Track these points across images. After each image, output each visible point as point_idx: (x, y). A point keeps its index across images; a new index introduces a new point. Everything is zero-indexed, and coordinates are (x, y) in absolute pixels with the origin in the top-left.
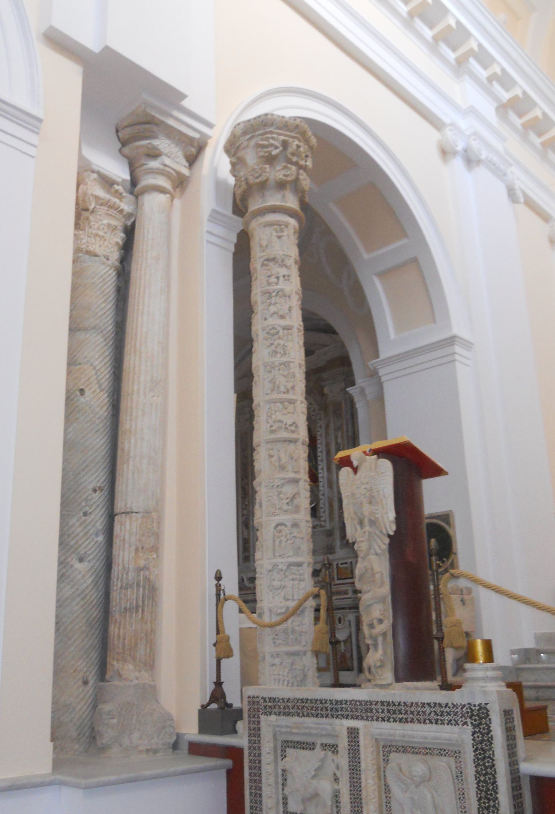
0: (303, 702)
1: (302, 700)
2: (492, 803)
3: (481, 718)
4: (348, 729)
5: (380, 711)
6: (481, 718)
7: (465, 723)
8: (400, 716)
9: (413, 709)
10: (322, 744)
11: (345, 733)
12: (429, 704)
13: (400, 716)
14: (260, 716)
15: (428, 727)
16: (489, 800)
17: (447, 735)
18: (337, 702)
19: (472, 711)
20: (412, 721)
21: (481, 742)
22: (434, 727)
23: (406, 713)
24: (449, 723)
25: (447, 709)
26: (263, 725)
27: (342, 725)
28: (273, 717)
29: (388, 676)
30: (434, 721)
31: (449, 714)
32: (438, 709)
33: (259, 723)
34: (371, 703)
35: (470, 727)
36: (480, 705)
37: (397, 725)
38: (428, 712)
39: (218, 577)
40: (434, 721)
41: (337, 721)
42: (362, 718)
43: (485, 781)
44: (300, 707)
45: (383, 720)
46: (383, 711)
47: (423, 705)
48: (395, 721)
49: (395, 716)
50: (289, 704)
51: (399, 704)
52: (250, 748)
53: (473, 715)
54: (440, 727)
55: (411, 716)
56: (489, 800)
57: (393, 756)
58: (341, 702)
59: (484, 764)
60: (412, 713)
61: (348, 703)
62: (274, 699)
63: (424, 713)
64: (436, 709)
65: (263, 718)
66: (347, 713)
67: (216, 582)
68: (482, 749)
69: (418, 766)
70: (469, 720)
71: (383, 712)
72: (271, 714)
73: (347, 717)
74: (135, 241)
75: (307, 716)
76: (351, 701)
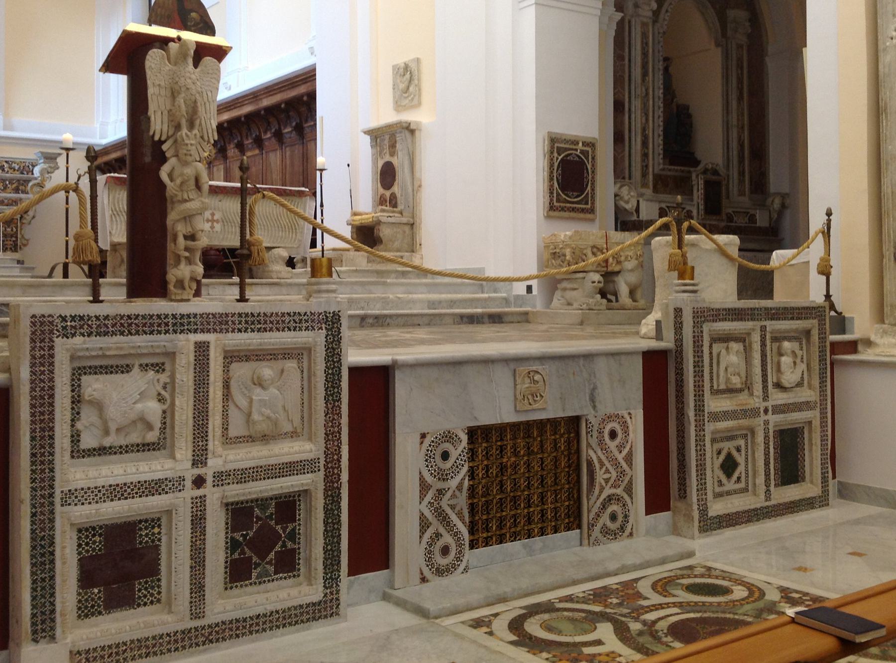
0: (131, 319)
1: (128, 316)
2: (336, 390)
3: (333, 323)
4: (196, 343)
5: (237, 322)
6: (333, 323)
7: (321, 328)
8: (259, 326)
9: (272, 319)
10: (141, 365)
11: (192, 348)
12: (289, 314)
13: (259, 326)
14: (55, 339)
15: (287, 334)
16: (334, 388)
17: (304, 340)
18: (182, 316)
19: (327, 317)
20: (271, 330)
21: (332, 343)
22: (292, 333)
23: (265, 322)
24: (307, 329)
25: (306, 317)
26: (57, 349)
27: (188, 340)
28: (78, 340)
29: (121, 294)
30: (292, 328)
31: (307, 321)
32: (297, 318)
33: (52, 348)
34: (227, 315)
35: (324, 331)
36: (334, 312)
37: (255, 335)
38: (287, 321)
39: (829, 214)
40: (292, 328)
41: (182, 337)
42: (215, 331)
43: (333, 374)
44: (126, 325)
45: (240, 331)
46: (240, 323)
47: (283, 314)
48: (253, 331)
49: (253, 326)
50: (107, 322)
51: (259, 315)
52: (32, 382)
53: (327, 321)
54: (298, 333)
55: (271, 325)
56: (334, 388)
57: (234, 366)
58: (189, 316)
59: (333, 360)
60: (271, 322)
61: (198, 317)
62: (81, 318)
63: (283, 322)
64: (295, 318)
65: (59, 342)
66: (195, 327)
67: (89, 164)
68: (332, 348)
69: (267, 371)
70: (324, 326)
71: (240, 323)
72: (74, 335)
73: (195, 331)
74: (866, 5)
75: (137, 333)
76: (201, 315)
